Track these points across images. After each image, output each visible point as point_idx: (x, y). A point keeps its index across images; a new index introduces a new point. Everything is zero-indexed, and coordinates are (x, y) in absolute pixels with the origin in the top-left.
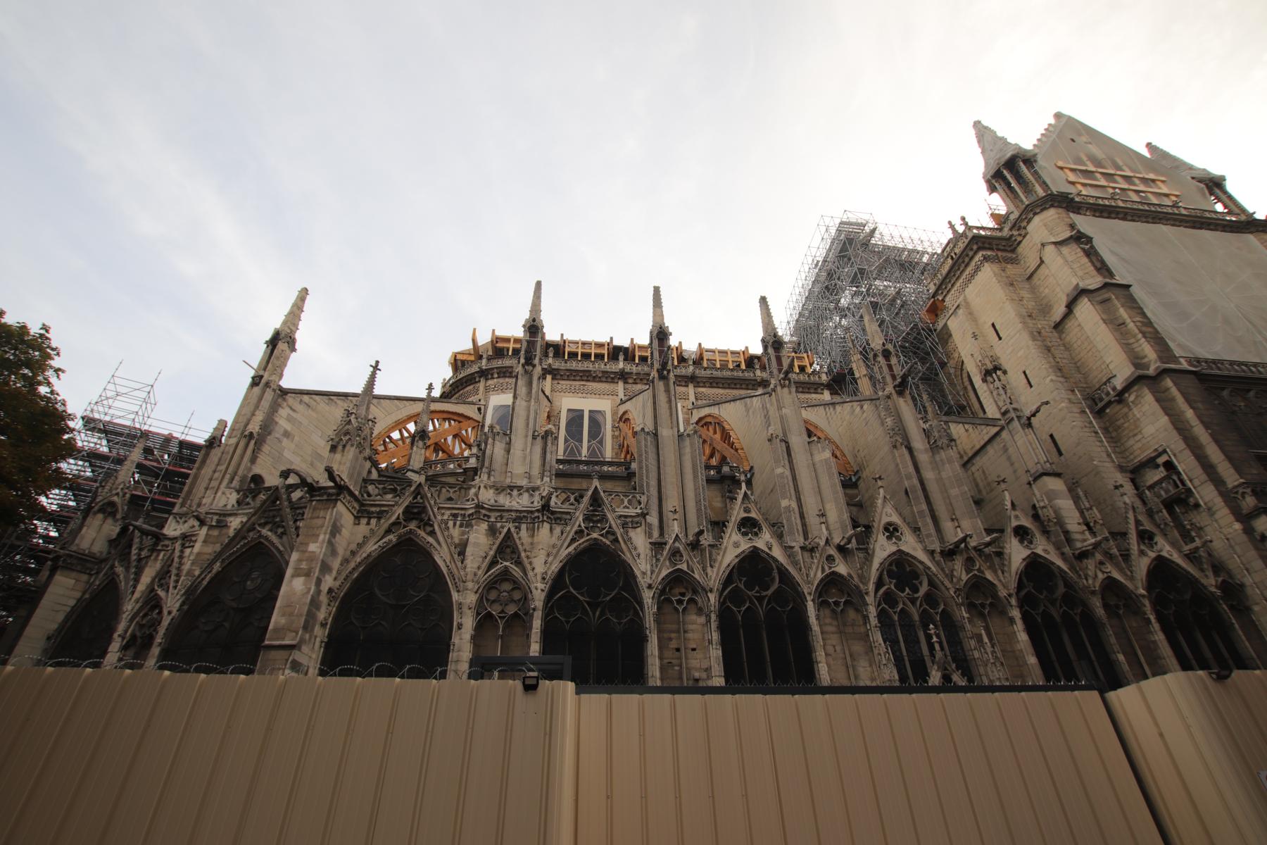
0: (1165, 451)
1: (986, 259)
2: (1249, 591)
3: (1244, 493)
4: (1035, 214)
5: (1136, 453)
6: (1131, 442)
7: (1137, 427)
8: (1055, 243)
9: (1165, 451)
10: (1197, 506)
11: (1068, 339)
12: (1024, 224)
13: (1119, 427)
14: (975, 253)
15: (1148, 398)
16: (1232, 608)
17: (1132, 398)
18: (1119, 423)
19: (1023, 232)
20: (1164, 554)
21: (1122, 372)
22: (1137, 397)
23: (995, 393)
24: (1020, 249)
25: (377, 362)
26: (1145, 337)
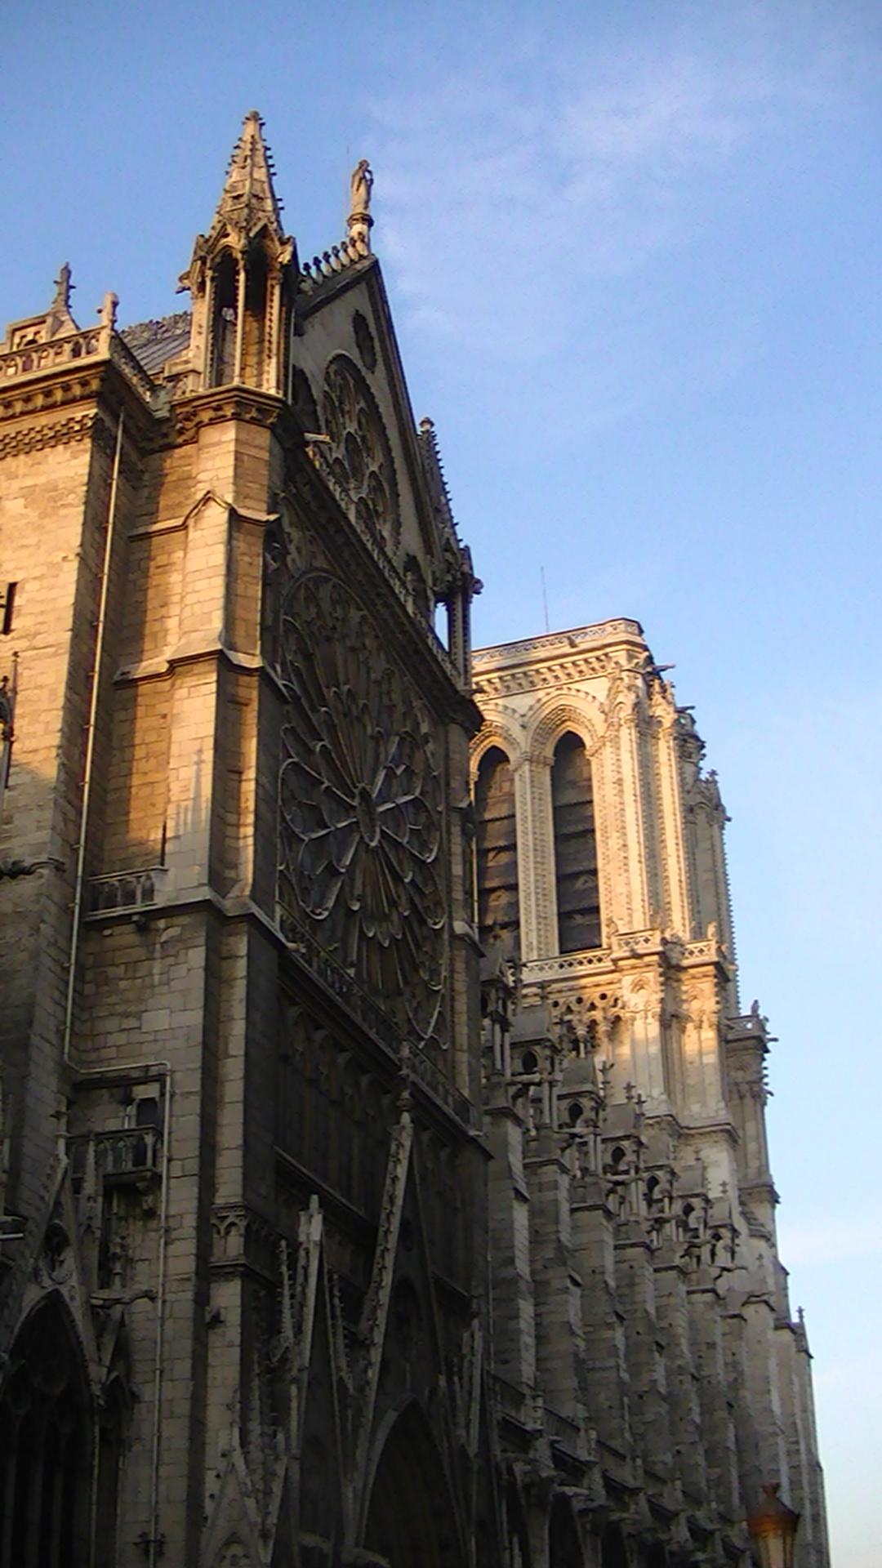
0: (160, 1079)
2: (141, 1410)
3: (233, 1224)
6: (112, 1024)
7: (140, 1000)
9: (160, 1079)
10: (151, 1214)
16: (103, 1431)
18: (111, 971)
20: (64, 1290)
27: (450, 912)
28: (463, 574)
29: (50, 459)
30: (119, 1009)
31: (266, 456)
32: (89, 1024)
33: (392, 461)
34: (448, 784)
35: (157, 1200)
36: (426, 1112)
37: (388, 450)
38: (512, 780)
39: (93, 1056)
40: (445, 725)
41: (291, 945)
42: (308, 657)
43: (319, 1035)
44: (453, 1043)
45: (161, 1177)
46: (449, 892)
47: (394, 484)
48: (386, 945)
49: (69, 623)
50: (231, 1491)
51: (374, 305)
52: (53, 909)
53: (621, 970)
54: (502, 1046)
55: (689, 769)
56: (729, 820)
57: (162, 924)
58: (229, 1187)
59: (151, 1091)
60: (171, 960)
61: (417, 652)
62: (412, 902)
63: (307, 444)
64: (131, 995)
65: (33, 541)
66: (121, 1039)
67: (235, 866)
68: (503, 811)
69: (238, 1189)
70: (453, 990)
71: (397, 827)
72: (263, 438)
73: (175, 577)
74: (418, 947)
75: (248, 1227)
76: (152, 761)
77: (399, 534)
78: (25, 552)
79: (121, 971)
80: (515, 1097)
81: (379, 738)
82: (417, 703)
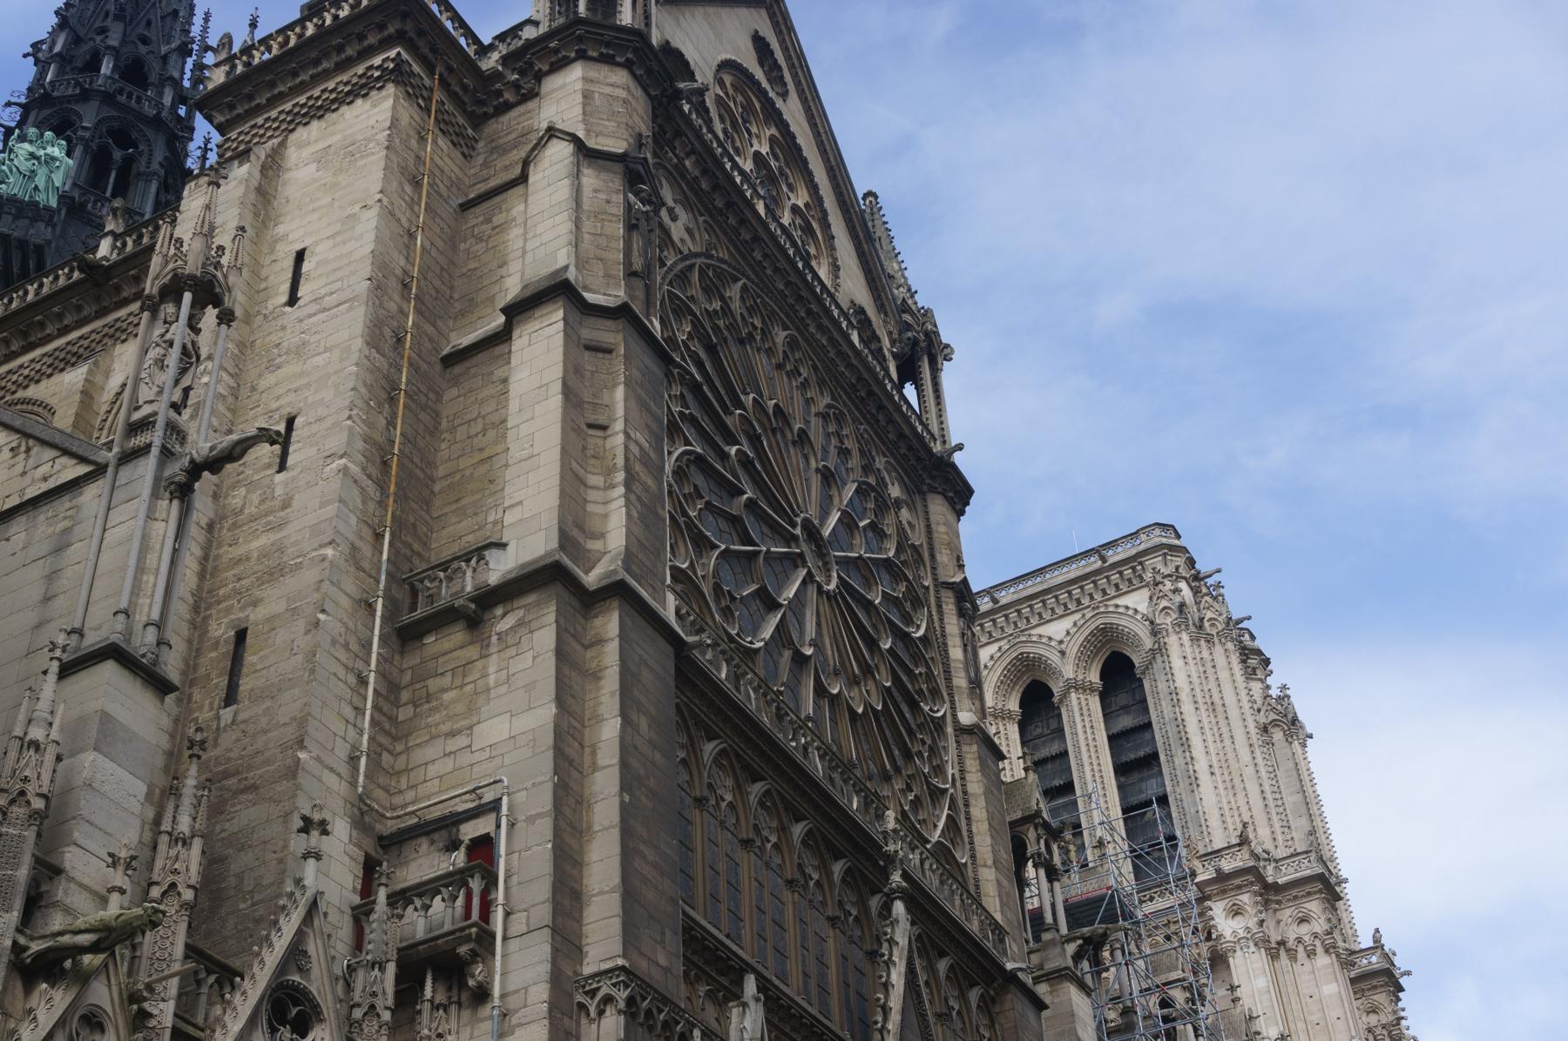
0: (495, 806)
1: (398, 74)
3: (608, 999)
4: (582, 56)
6: (431, 752)
7: (471, 709)
9: (495, 806)
10: (481, 995)
13: (429, 698)
14: (385, 44)
18: (433, 684)
23: (154, 353)
26: (628, 484)
27: (953, 703)
28: (927, 334)
29: (347, 116)
30: (445, 728)
32: (404, 757)
33: (820, 200)
34: (933, 557)
35: (490, 974)
37: (813, 188)
38: (1060, 715)
39: (410, 796)
40: (922, 493)
41: (690, 639)
42: (711, 349)
43: (756, 789)
44: (973, 857)
45: (493, 936)
46: (948, 679)
47: (826, 226)
48: (860, 711)
49: (366, 270)
51: (776, 25)
52: (345, 602)
53: (1208, 898)
54: (1053, 905)
55: (1256, 687)
56: (1311, 737)
58: (603, 944)
60: (512, 651)
61: (871, 393)
62: (894, 672)
63: (678, 95)
64: (460, 708)
65: (328, 200)
66: (447, 765)
67: (602, 536)
68: (1055, 748)
69: (617, 947)
70: (965, 793)
71: (869, 583)
72: (620, 77)
73: (515, 233)
74: (911, 733)
75: (630, 1001)
76: (491, 433)
77: (837, 277)
78: (316, 216)
79: (448, 679)
80: (1077, 957)
81: (828, 478)
82: (880, 463)
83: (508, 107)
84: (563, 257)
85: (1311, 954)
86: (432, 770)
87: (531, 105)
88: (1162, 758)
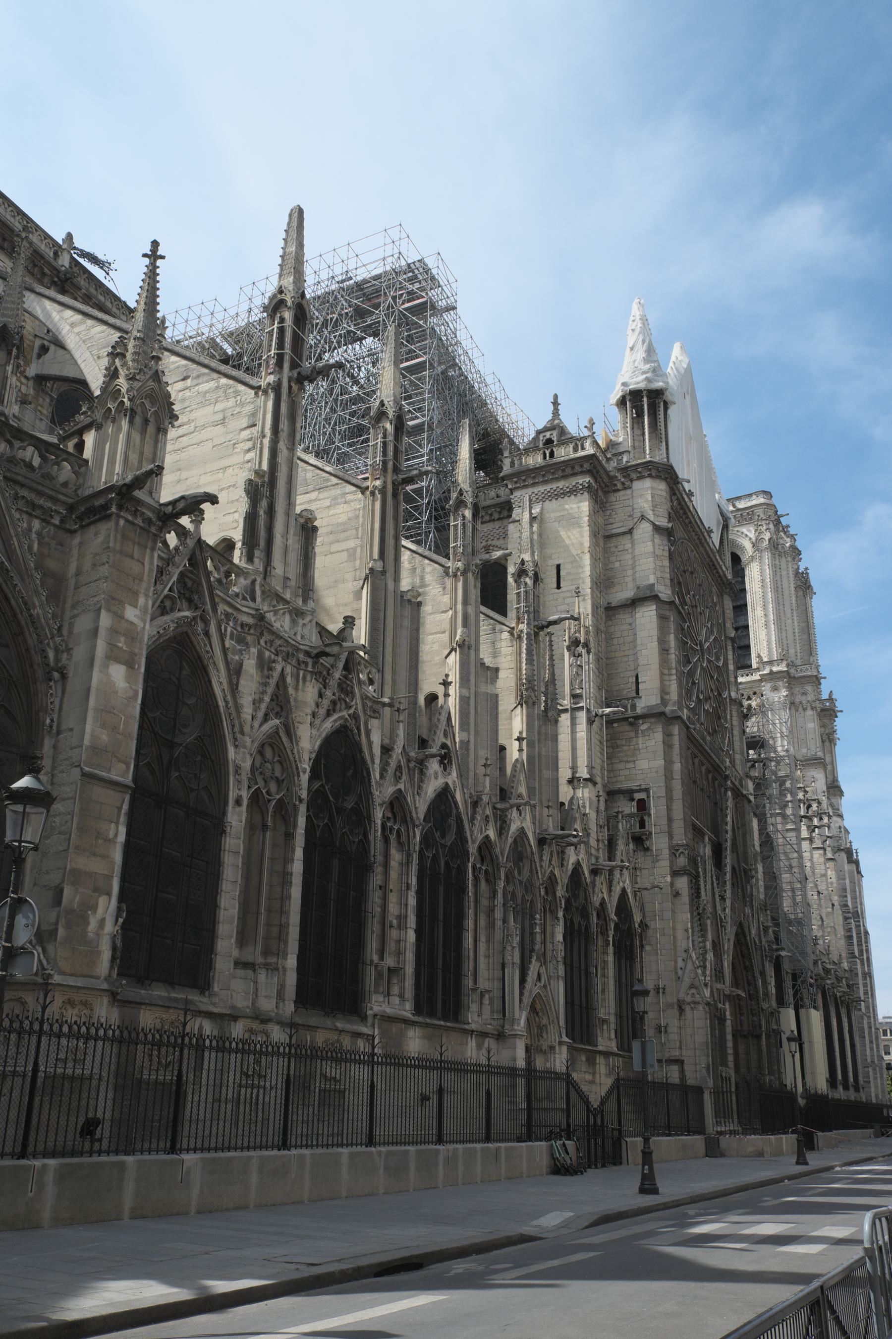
0: (647, 790)
1: (589, 488)
4: (650, 476)
5: (619, 778)
6: (621, 766)
7: (633, 755)
8: (654, 524)
9: (647, 790)
11: (612, 629)
12: (634, 475)
13: (618, 747)
15: (658, 735)
17: (644, 727)
19: (628, 484)
21: (648, 700)
22: (649, 729)
24: (613, 497)
25: (155, 244)
30: (625, 759)
31: (664, 494)
36: (732, 790)
46: (728, 679)
50: (690, 966)
57: (641, 721)
59: (642, 795)
60: (647, 738)
66: (627, 773)
79: (624, 742)
83: (618, 490)
84: (652, 580)
85: (805, 709)
86: (622, 773)
87: (629, 492)
88: (749, 608)
